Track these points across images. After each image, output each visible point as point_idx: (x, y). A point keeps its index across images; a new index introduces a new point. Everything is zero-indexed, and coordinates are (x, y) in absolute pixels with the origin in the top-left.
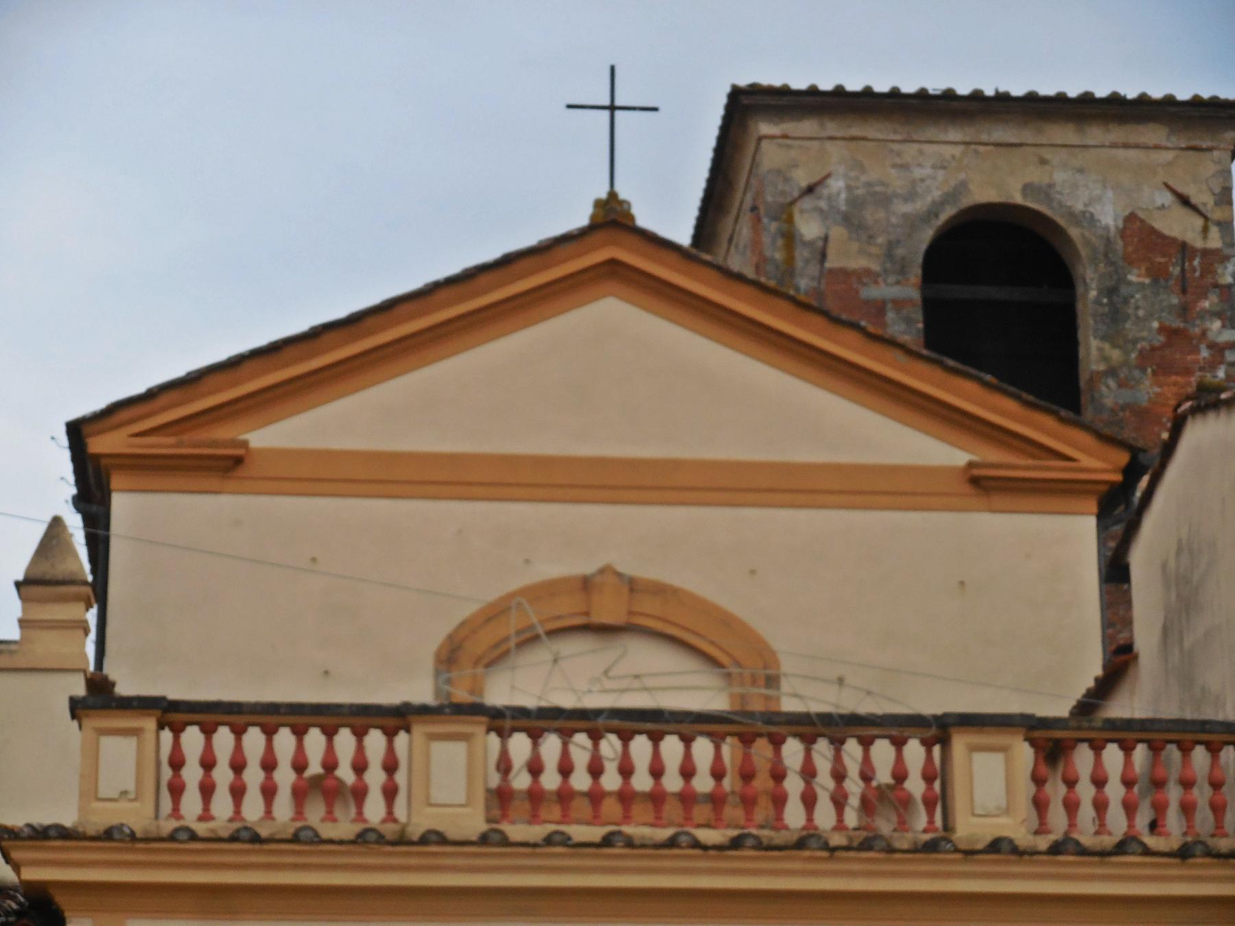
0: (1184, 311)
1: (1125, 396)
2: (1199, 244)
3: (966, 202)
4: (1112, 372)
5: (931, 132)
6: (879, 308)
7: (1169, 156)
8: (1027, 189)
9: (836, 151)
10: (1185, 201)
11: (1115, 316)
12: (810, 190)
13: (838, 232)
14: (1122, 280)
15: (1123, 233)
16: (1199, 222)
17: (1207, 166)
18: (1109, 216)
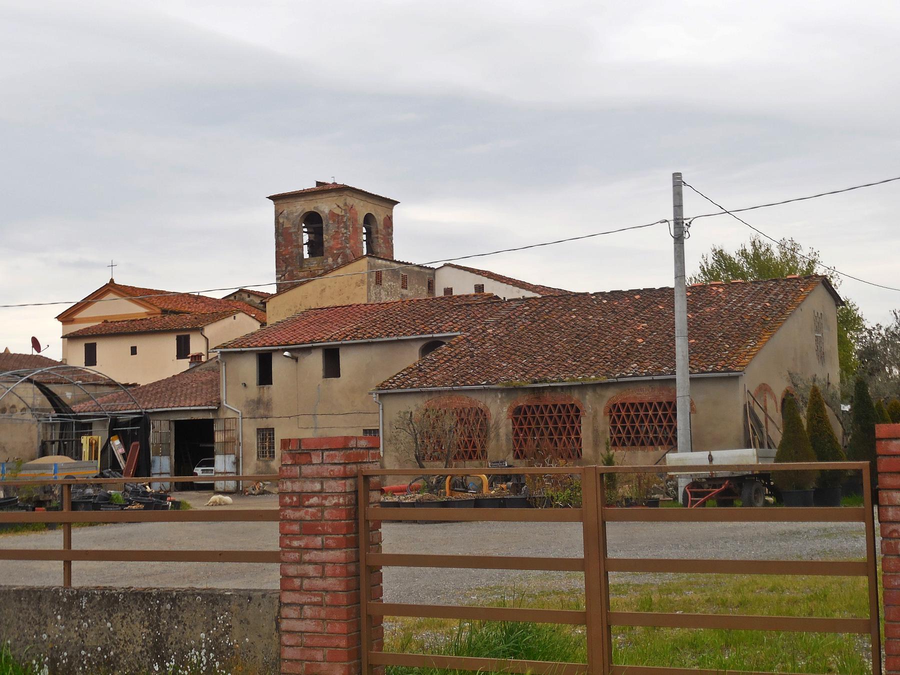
0: (338, 227)
1: (329, 245)
2: (340, 214)
3: (305, 212)
4: (326, 241)
5: (299, 199)
6: (291, 233)
7: (336, 198)
8: (314, 207)
9: (284, 205)
10: (338, 206)
11: (327, 230)
12: (281, 213)
13: (285, 220)
14: (328, 223)
15: (329, 214)
16: (340, 210)
17: (342, 199)
18: (327, 211)
